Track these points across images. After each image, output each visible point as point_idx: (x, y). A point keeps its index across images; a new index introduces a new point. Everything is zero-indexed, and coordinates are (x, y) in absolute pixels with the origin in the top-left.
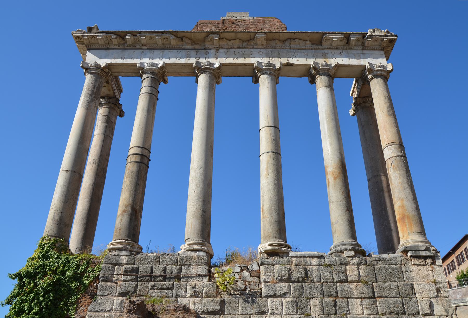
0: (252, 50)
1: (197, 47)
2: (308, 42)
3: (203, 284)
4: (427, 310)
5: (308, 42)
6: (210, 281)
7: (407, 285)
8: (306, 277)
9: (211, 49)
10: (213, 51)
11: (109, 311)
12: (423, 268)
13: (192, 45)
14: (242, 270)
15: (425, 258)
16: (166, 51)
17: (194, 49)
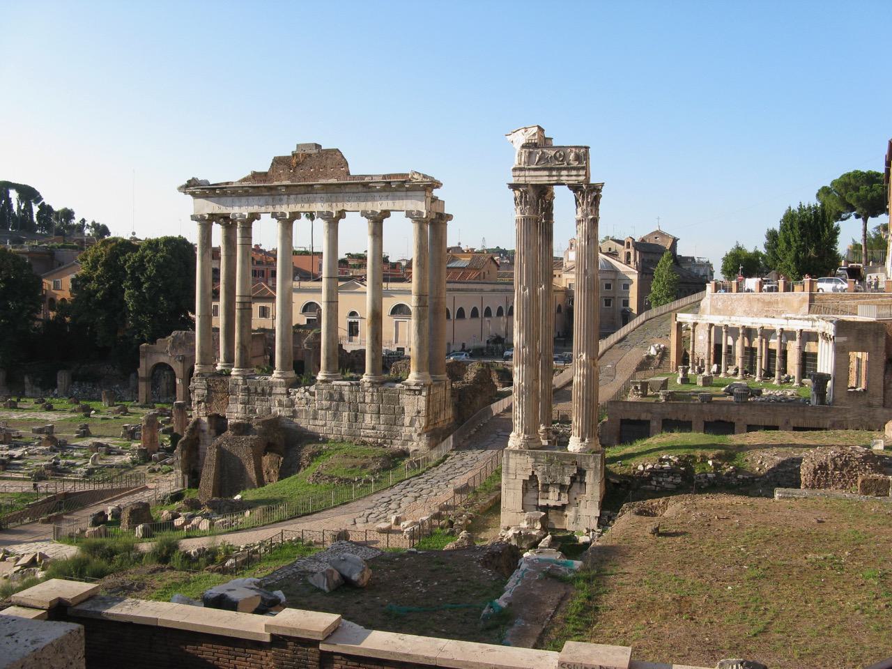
0: (315, 195)
1: (273, 192)
2: (359, 186)
3: (284, 399)
4: (408, 425)
5: (359, 186)
6: (288, 397)
7: (400, 408)
8: (341, 399)
9: (284, 195)
10: (286, 197)
11: (237, 412)
12: (411, 397)
13: (268, 191)
14: (305, 391)
15: (415, 390)
16: (251, 198)
17: (272, 195)
